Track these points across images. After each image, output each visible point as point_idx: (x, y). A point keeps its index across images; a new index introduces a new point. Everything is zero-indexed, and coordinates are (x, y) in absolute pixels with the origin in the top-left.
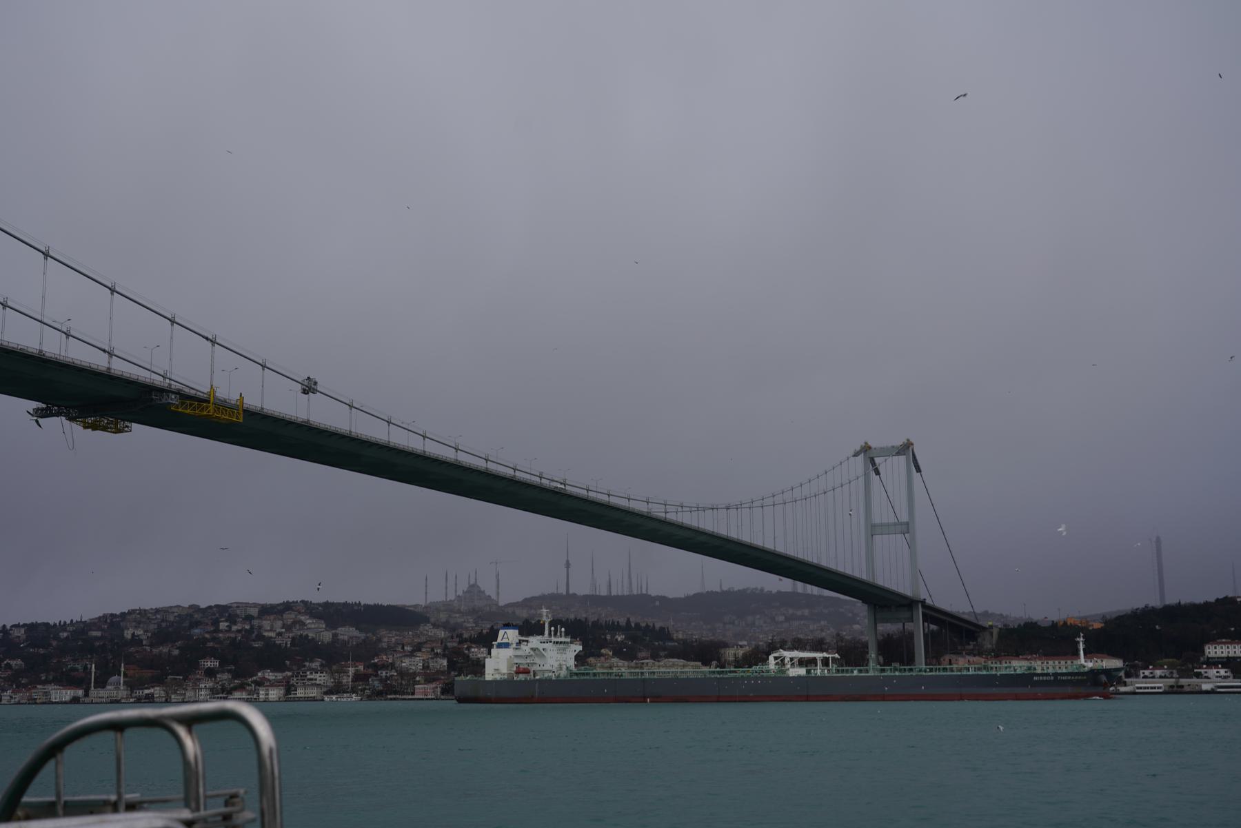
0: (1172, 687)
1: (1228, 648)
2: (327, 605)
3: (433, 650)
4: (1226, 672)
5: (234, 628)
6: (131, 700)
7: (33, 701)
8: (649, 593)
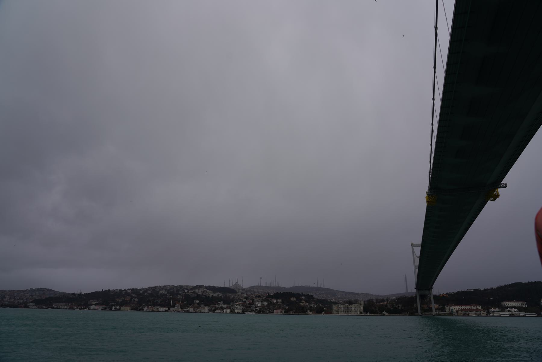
0: (511, 314)
2: (209, 286)
3: (260, 300)
5: (189, 292)
6: (183, 312)
7: (153, 311)
8: (281, 286)
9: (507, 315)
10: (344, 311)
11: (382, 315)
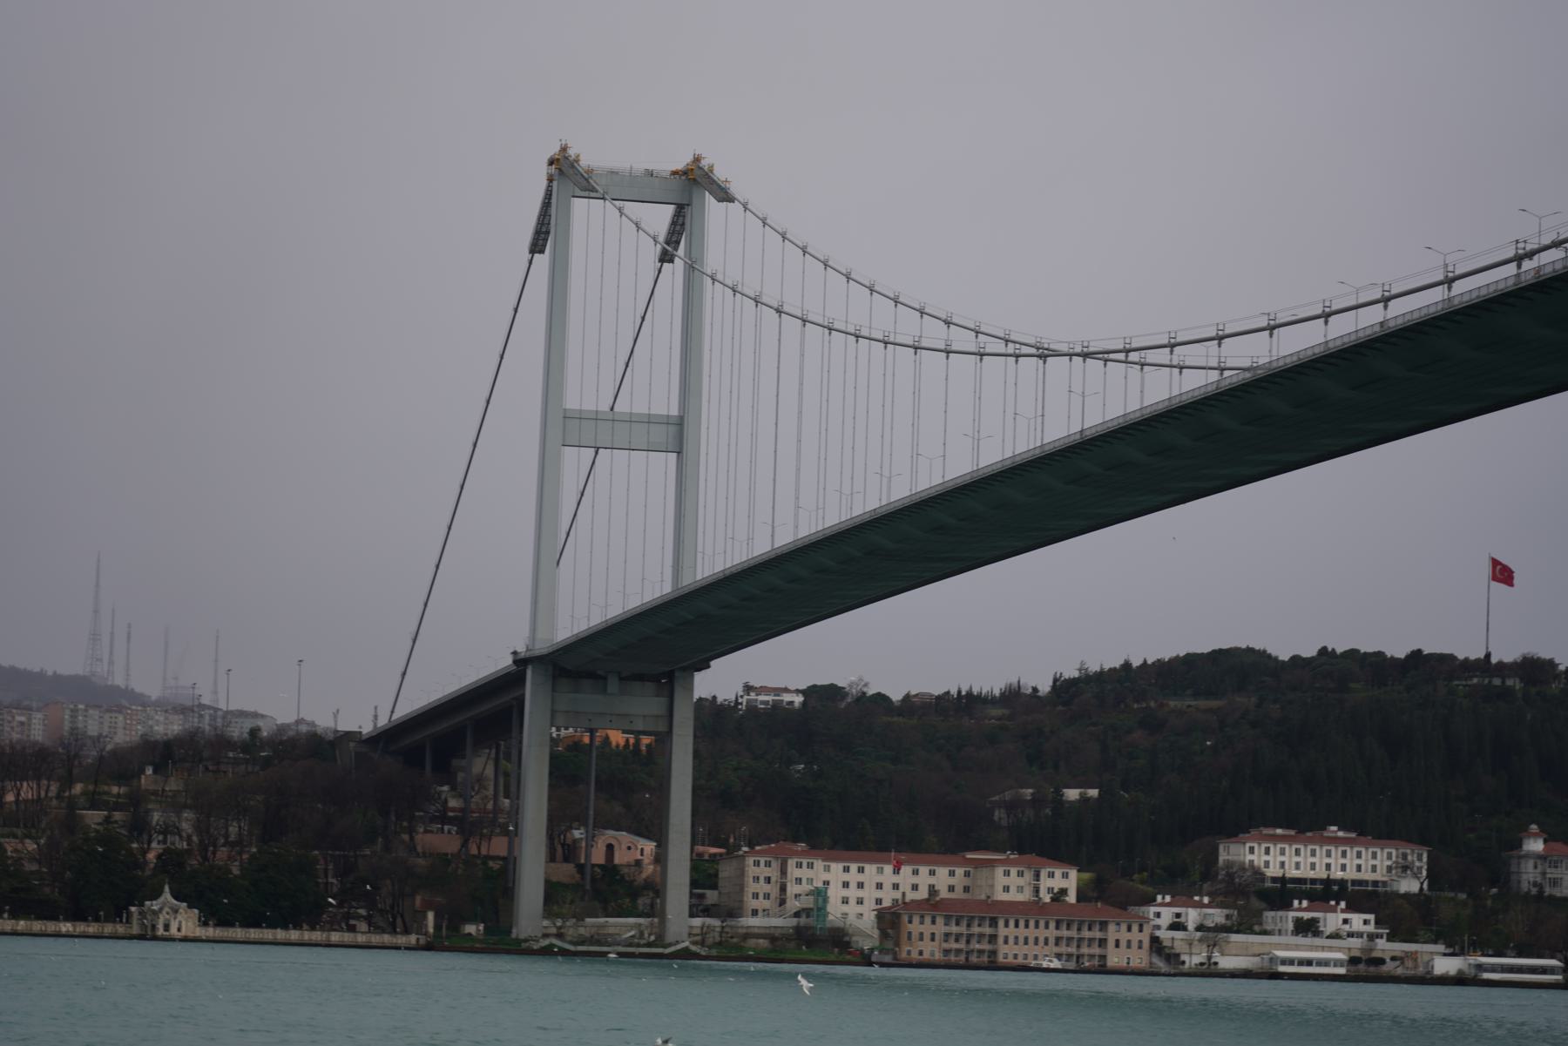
1: (1344, 854)
4: (1366, 922)
9: (1325, 963)
11: (135, 930)
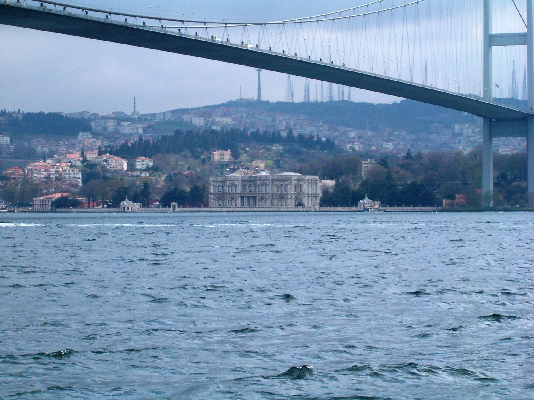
10: (242, 198)
